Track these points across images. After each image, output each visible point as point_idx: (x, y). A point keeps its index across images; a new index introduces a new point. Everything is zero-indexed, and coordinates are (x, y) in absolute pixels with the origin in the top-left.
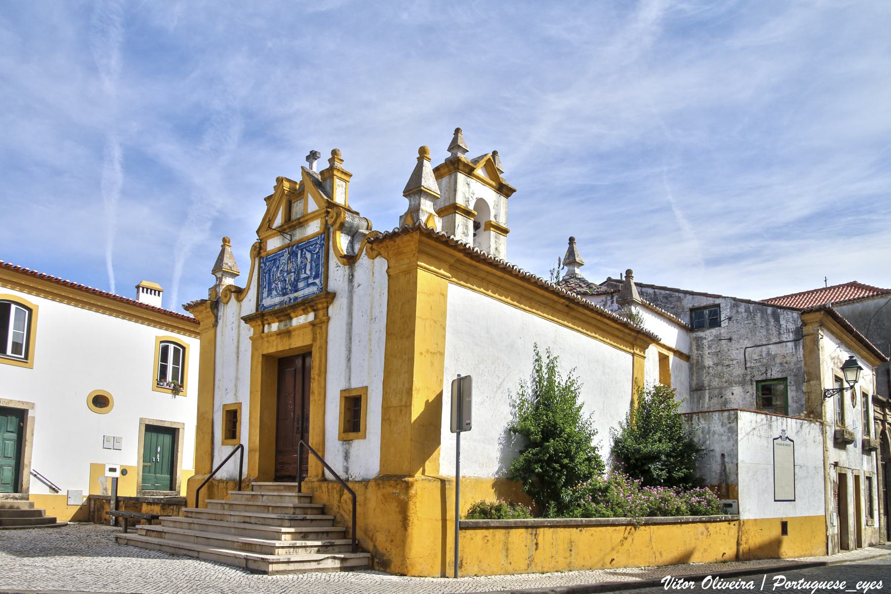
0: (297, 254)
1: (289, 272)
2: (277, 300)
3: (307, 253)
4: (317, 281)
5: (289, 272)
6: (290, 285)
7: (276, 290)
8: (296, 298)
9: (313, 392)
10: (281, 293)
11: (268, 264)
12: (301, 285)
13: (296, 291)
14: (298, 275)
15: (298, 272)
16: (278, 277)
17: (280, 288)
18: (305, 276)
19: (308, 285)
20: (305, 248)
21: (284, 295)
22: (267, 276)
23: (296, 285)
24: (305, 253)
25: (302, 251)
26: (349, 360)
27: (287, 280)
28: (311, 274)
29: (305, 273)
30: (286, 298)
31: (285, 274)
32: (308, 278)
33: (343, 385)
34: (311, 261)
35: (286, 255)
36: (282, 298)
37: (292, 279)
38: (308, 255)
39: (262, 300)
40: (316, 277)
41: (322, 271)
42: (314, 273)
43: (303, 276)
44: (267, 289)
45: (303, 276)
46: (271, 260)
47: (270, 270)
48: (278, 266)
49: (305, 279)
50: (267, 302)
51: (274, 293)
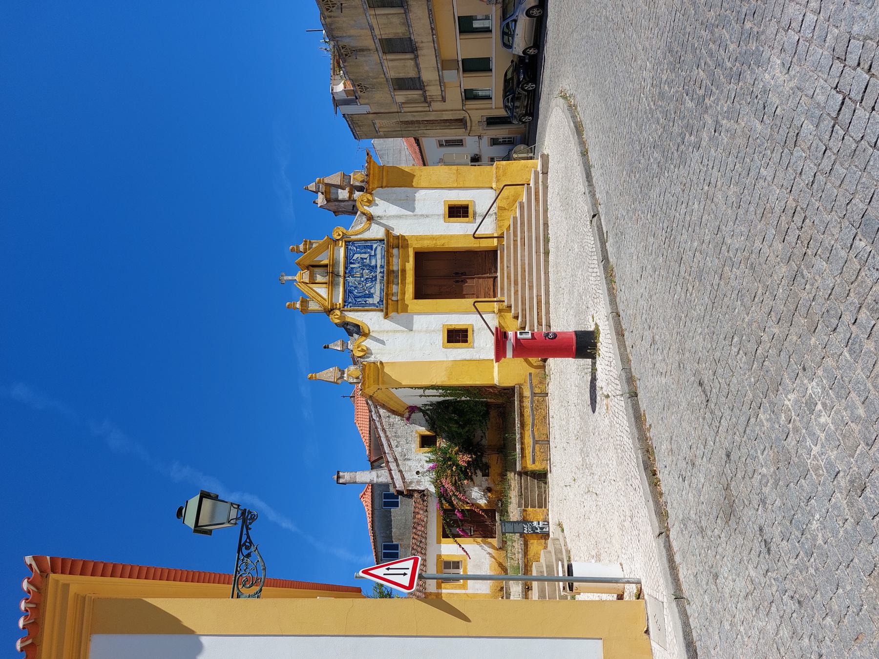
0: (352, 268)
1: (362, 276)
2: (378, 286)
3: (354, 258)
4: (374, 247)
5: (362, 276)
6: (371, 273)
7: (371, 288)
8: (382, 267)
9: (443, 245)
10: (374, 283)
11: (350, 300)
12: (373, 263)
13: (376, 266)
14: (365, 266)
15: (364, 266)
16: (363, 286)
17: (371, 284)
18: (368, 259)
19: (375, 255)
20: (350, 260)
21: (376, 280)
22: (358, 300)
23: (373, 267)
24: (354, 260)
25: (351, 263)
26: (427, 216)
27: (367, 277)
28: (369, 253)
29: (366, 259)
30: (379, 277)
31: (362, 279)
32: (370, 256)
33: (442, 221)
34: (360, 253)
35: (350, 279)
36: (378, 280)
37: (367, 271)
38: (356, 256)
39: (374, 305)
40: (371, 247)
41: (367, 245)
42: (369, 250)
43: (368, 261)
44: (367, 299)
45: (368, 261)
46: (349, 295)
47: (356, 297)
48: (355, 287)
49: (370, 259)
50: (376, 299)
51: (372, 291)
